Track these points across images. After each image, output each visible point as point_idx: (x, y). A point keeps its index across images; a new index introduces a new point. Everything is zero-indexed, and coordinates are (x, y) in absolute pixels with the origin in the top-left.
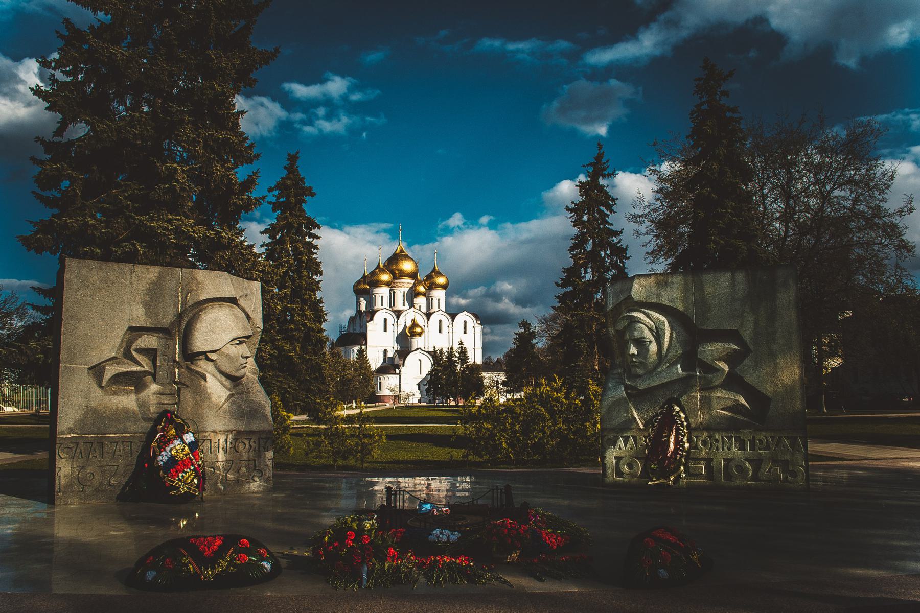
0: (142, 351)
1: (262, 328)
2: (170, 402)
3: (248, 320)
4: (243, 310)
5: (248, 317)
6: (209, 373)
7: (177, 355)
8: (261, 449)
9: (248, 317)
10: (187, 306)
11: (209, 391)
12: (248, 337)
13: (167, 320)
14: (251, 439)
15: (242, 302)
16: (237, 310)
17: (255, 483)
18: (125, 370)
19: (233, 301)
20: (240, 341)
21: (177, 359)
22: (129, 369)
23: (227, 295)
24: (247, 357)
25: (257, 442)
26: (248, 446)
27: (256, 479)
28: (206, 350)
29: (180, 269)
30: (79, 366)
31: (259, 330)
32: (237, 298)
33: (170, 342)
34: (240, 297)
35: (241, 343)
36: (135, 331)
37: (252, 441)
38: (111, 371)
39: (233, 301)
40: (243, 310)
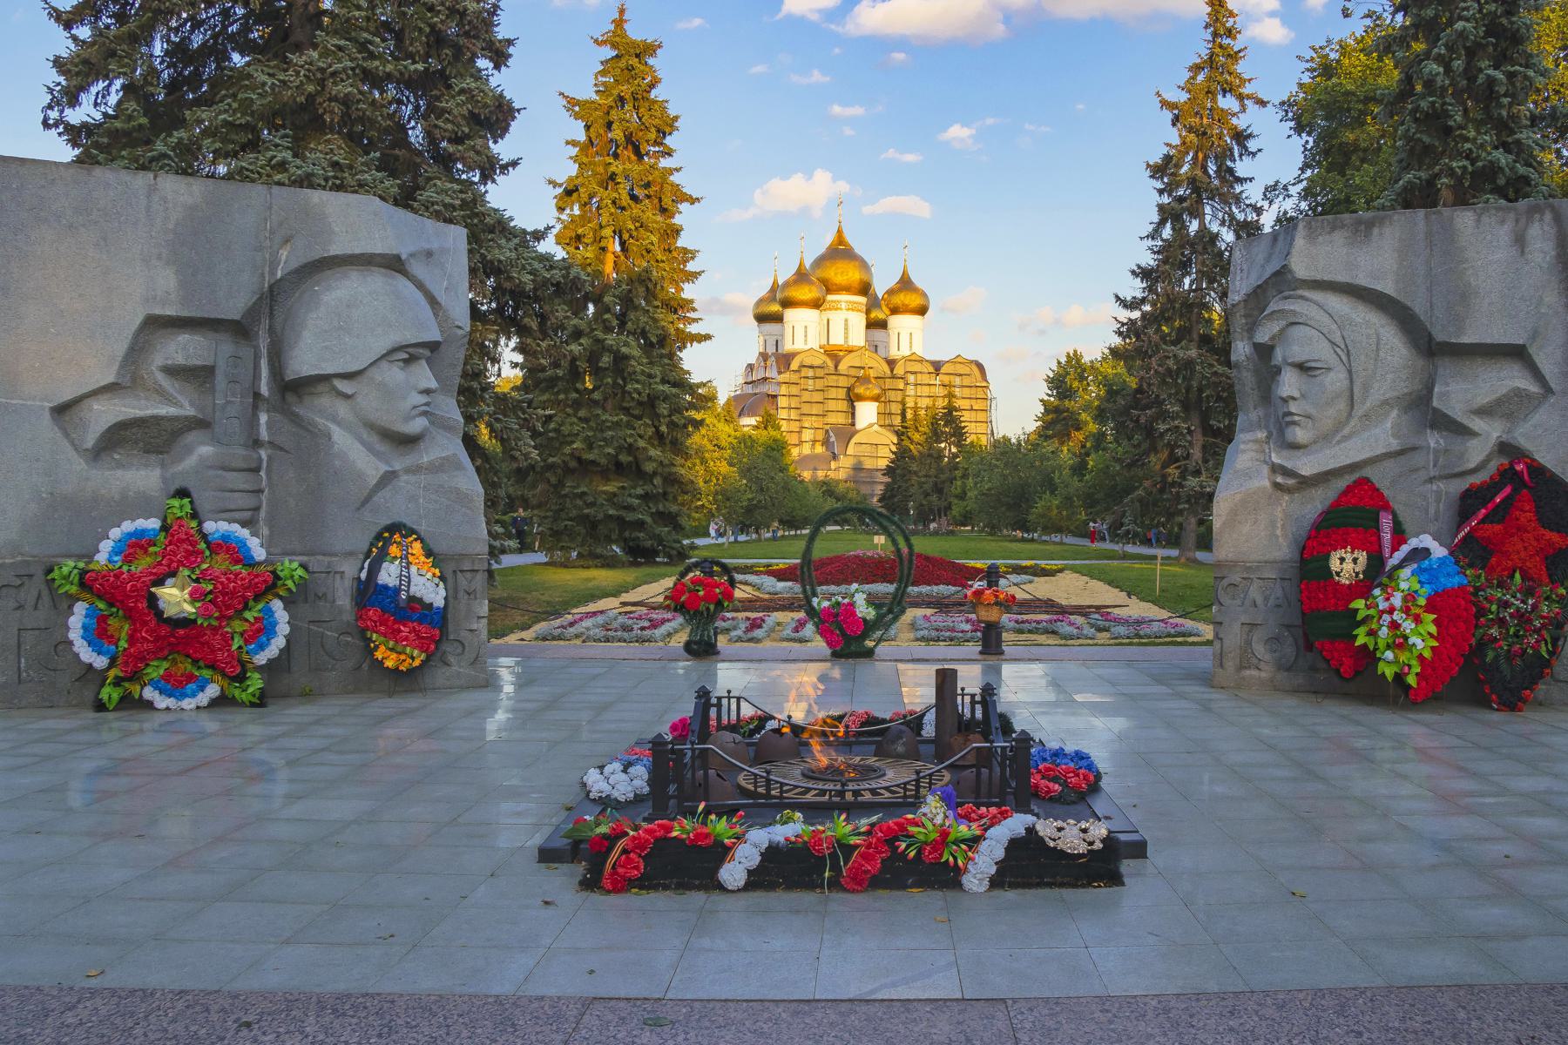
0: (172, 371)
1: (468, 329)
3: (433, 308)
4: (420, 286)
5: (433, 301)
6: (339, 424)
9: (433, 301)
12: (434, 346)
13: (234, 307)
15: (418, 269)
18: (139, 413)
19: (394, 264)
20: (408, 354)
21: (264, 390)
22: (149, 412)
23: (379, 248)
24: (427, 392)
31: (460, 332)
32: (404, 257)
33: (246, 352)
34: (412, 255)
35: (408, 361)
38: (105, 414)
39: (394, 264)
40: (420, 286)
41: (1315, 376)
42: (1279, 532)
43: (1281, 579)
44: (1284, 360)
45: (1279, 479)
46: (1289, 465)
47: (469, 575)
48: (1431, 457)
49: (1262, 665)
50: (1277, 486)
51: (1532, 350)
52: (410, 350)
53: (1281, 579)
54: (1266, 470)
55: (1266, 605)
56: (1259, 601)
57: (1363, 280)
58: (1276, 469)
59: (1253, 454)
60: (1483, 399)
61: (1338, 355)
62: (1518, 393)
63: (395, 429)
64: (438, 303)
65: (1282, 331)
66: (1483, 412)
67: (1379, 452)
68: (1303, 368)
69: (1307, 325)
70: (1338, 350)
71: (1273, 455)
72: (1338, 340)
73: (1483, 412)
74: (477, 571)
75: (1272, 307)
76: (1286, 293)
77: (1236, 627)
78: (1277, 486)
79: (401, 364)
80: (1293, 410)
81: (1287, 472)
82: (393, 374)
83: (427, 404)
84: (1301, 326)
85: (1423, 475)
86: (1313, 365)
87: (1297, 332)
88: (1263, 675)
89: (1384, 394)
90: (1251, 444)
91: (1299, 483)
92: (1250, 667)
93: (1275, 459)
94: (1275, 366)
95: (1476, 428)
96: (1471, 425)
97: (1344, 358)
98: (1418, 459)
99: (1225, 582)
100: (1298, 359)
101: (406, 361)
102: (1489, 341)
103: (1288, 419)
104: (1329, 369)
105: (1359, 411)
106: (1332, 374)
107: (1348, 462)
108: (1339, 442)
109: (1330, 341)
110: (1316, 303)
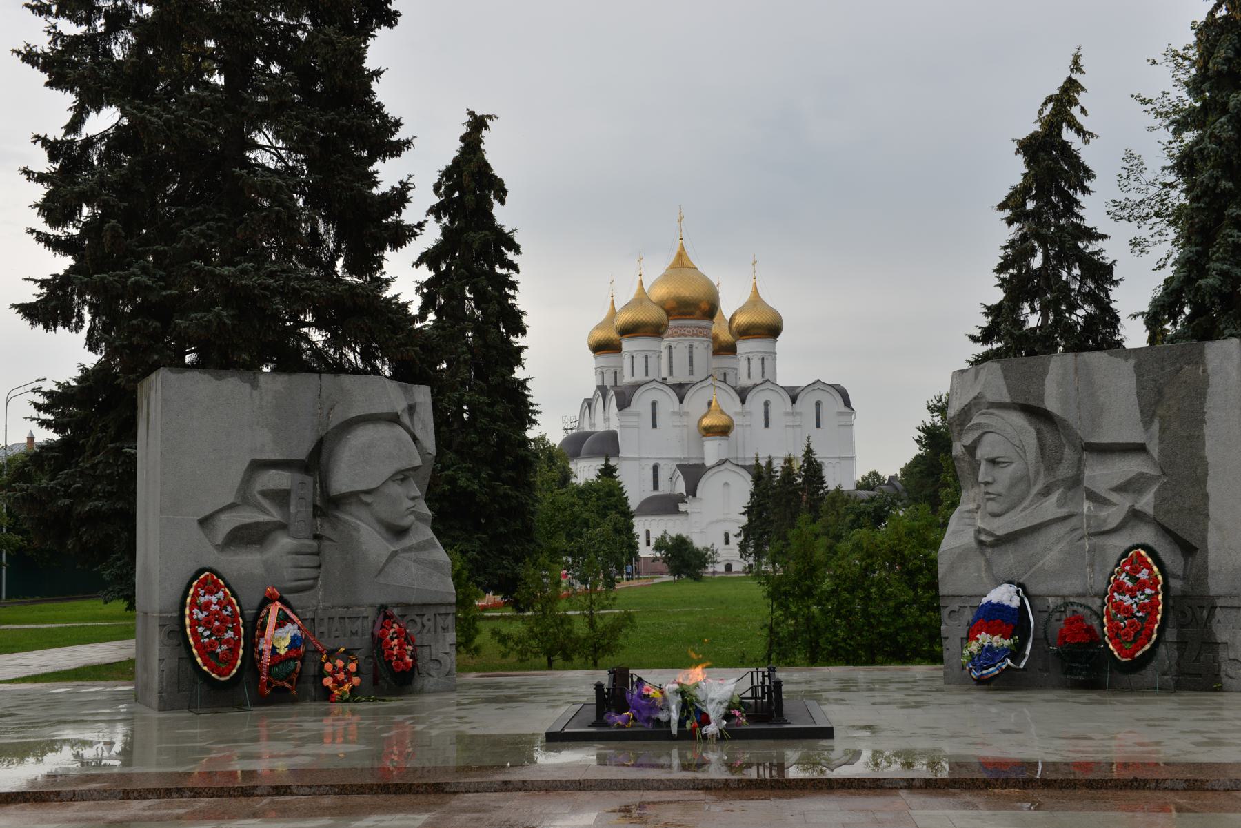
1: (435, 455)
2: (311, 565)
5: (415, 439)
7: (318, 498)
8: (439, 629)
9: (415, 439)
10: (330, 428)
11: (364, 547)
12: (415, 469)
14: (423, 615)
16: (399, 430)
17: (431, 678)
18: (247, 521)
19: (394, 419)
20: (403, 476)
22: (253, 520)
23: (385, 409)
24: (414, 499)
25: (433, 620)
26: (420, 625)
27: (433, 673)
28: (358, 488)
29: (318, 375)
30: (186, 517)
36: (258, 466)
37: (425, 618)
38: (228, 522)
39: (394, 419)
42: (983, 574)
45: (983, 538)
46: (988, 528)
47: (443, 617)
48: (1085, 520)
50: (981, 543)
51: (1149, 447)
52: (405, 473)
54: (971, 532)
58: (979, 531)
59: (967, 521)
60: (1117, 482)
62: (1141, 476)
63: (396, 524)
64: (417, 439)
65: (980, 437)
66: (1119, 489)
67: (1048, 519)
68: (993, 462)
70: (1018, 449)
71: (979, 521)
72: (1017, 443)
73: (1120, 489)
74: (449, 614)
75: (975, 421)
76: (982, 411)
78: (981, 543)
79: (399, 482)
81: (989, 533)
82: (396, 489)
83: (414, 507)
84: (991, 434)
85: (1078, 533)
87: (988, 437)
90: (966, 514)
93: (979, 524)
95: (1115, 501)
96: (1111, 499)
98: (1073, 522)
100: (991, 456)
101: (402, 480)
102: (1121, 441)
103: (987, 496)
104: (1012, 463)
106: (1013, 466)
107: (1028, 525)
108: (1022, 511)
110: (1002, 418)
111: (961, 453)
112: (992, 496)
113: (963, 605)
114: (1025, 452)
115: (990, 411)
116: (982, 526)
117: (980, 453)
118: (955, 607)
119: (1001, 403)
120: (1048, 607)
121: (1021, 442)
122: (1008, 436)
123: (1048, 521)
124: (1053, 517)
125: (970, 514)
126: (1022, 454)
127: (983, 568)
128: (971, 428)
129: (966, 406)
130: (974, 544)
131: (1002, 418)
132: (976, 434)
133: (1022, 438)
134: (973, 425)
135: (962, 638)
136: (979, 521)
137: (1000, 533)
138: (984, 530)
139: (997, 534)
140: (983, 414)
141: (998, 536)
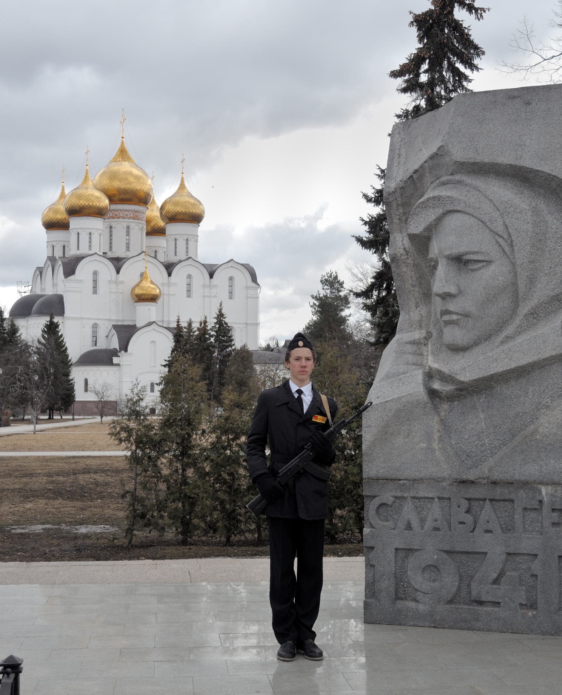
41: (475, 270)
42: (435, 446)
43: (440, 498)
44: (440, 252)
45: (437, 386)
46: (446, 370)
49: (420, 596)
50: (433, 394)
53: (440, 498)
54: (419, 375)
55: (422, 528)
56: (415, 524)
57: (528, 162)
58: (430, 375)
59: (411, 358)
61: (500, 246)
65: (439, 220)
67: (547, 355)
69: (465, 213)
70: (500, 240)
71: (430, 358)
72: (500, 229)
75: (430, 194)
76: (444, 179)
77: (390, 553)
80: (451, 309)
81: (445, 378)
86: (472, 257)
88: (421, 607)
89: (553, 289)
90: (409, 346)
91: (457, 390)
92: (405, 599)
93: (432, 363)
94: (431, 260)
97: (507, 249)
99: (376, 502)
100: (455, 251)
103: (446, 318)
104: (489, 262)
105: (524, 309)
106: (492, 267)
107: (513, 365)
108: (502, 342)
109: (491, 230)
110: (476, 188)
111: (402, 251)
112: (455, 317)
113: (399, 494)
114: (511, 245)
115: (457, 177)
116: (435, 366)
117: (435, 249)
118: (387, 497)
119: (475, 164)
120: (541, 502)
121: (506, 227)
122: (486, 219)
123: (545, 360)
124: (554, 353)
125: (415, 348)
126: (507, 249)
127: (436, 436)
128: (425, 206)
129: (416, 172)
130: (423, 395)
131: (476, 188)
132: (431, 216)
133: (507, 222)
134: (428, 200)
135: (397, 549)
136: (430, 358)
137: (466, 377)
138: (440, 372)
139: (462, 379)
140: (444, 184)
141: (463, 382)
